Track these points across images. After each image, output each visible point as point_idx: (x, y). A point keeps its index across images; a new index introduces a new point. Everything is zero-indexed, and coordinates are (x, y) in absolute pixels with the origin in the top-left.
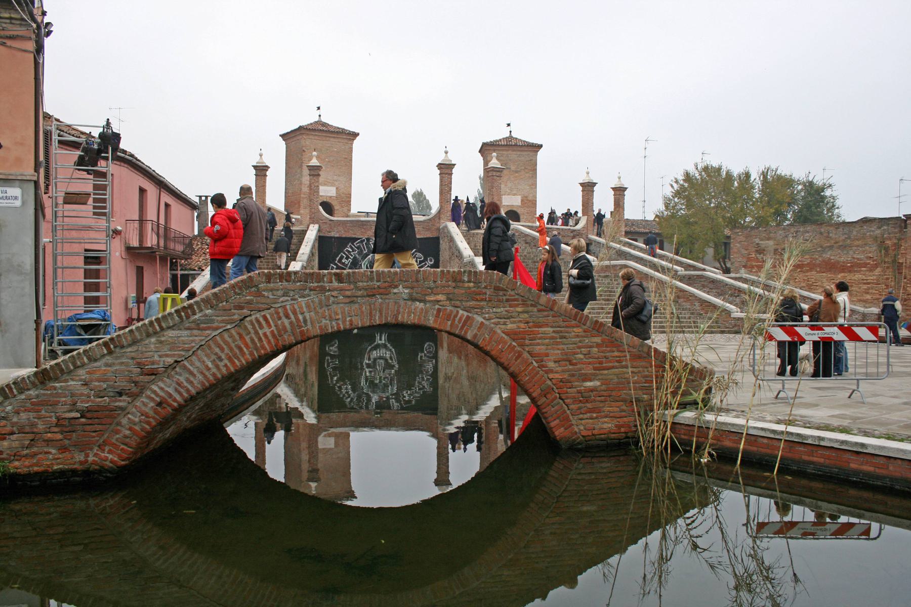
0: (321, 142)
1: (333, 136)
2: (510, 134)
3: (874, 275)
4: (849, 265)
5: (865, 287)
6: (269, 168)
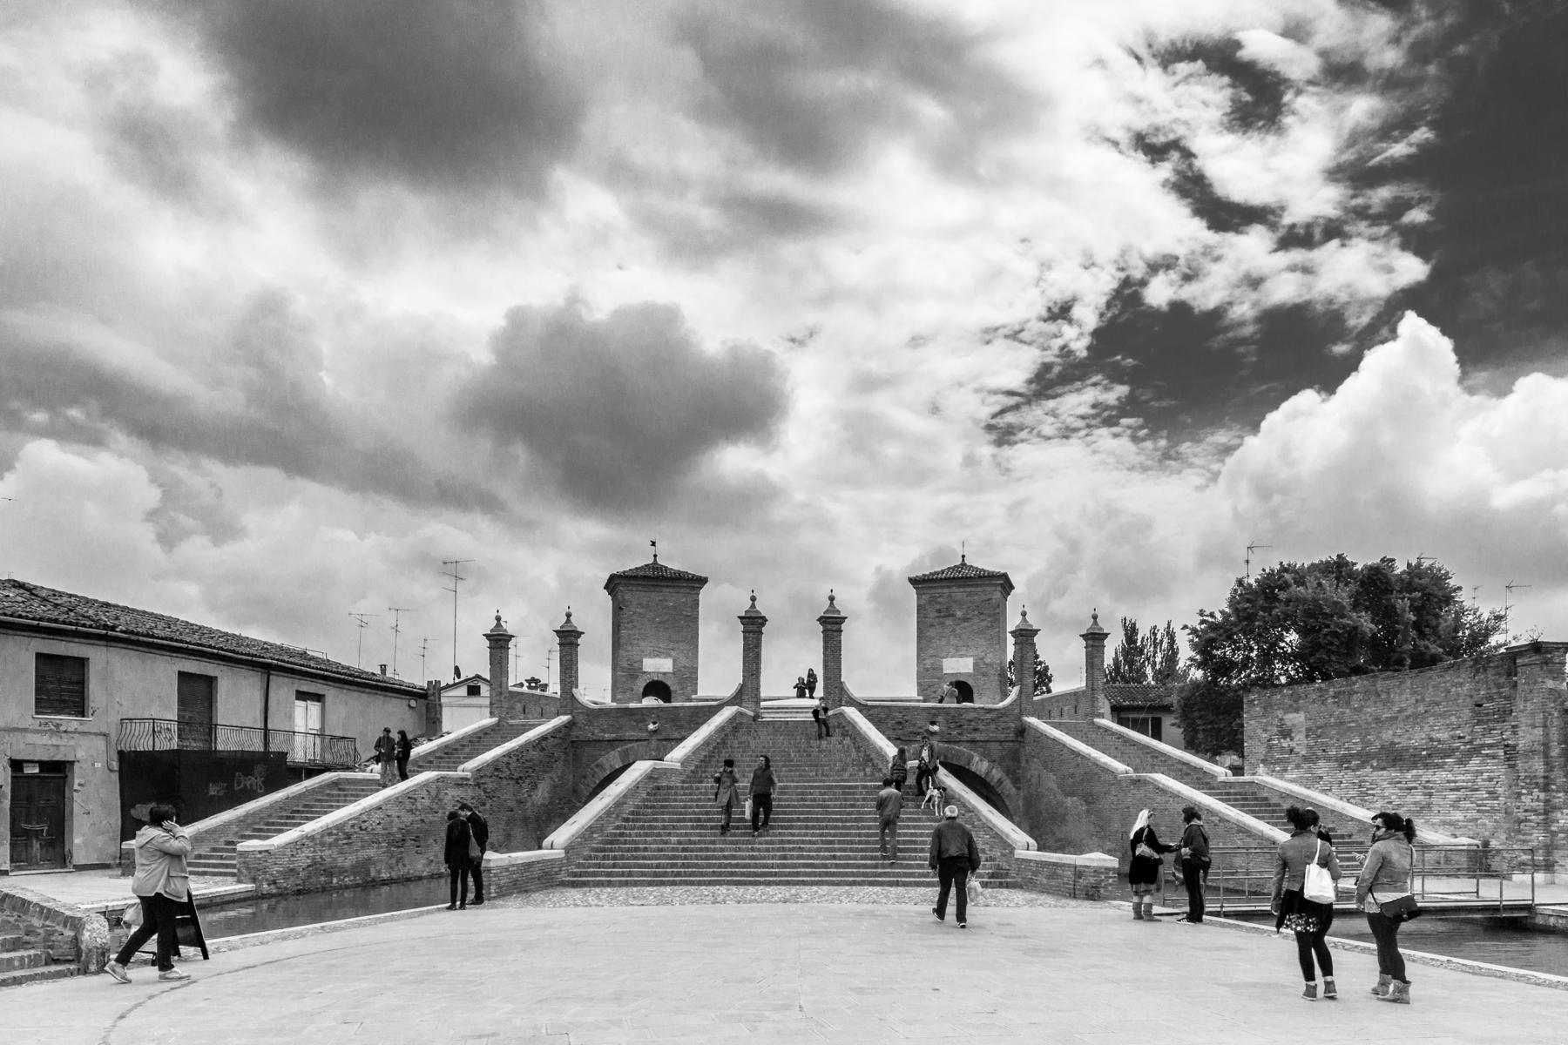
0: (648, 594)
1: (666, 584)
2: (963, 560)
3: (1468, 772)
4: (1424, 753)
5: (1452, 796)
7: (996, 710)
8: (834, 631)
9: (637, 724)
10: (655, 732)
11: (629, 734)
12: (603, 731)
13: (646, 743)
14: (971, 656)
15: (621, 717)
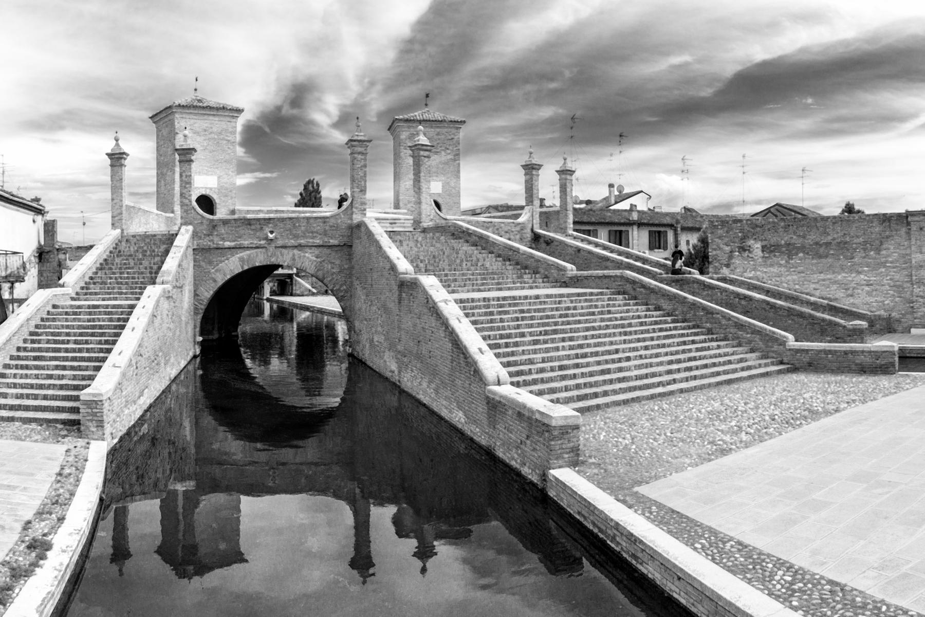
1: (212, 113)
6: (128, 155)
7: (520, 224)
8: (425, 157)
9: (255, 234)
10: (271, 240)
11: (246, 243)
12: (223, 239)
13: (264, 250)
14: (440, 181)
15: (239, 227)
